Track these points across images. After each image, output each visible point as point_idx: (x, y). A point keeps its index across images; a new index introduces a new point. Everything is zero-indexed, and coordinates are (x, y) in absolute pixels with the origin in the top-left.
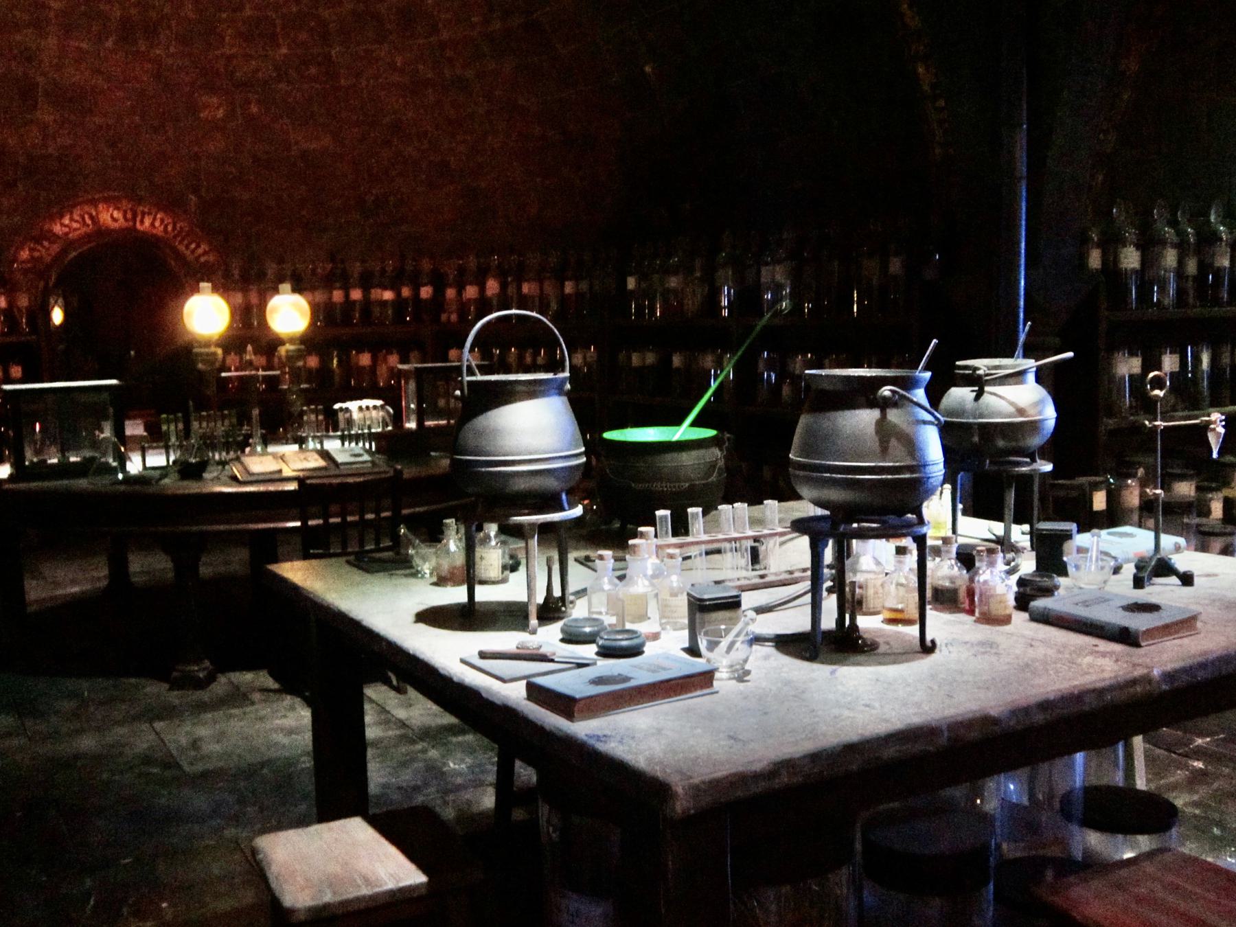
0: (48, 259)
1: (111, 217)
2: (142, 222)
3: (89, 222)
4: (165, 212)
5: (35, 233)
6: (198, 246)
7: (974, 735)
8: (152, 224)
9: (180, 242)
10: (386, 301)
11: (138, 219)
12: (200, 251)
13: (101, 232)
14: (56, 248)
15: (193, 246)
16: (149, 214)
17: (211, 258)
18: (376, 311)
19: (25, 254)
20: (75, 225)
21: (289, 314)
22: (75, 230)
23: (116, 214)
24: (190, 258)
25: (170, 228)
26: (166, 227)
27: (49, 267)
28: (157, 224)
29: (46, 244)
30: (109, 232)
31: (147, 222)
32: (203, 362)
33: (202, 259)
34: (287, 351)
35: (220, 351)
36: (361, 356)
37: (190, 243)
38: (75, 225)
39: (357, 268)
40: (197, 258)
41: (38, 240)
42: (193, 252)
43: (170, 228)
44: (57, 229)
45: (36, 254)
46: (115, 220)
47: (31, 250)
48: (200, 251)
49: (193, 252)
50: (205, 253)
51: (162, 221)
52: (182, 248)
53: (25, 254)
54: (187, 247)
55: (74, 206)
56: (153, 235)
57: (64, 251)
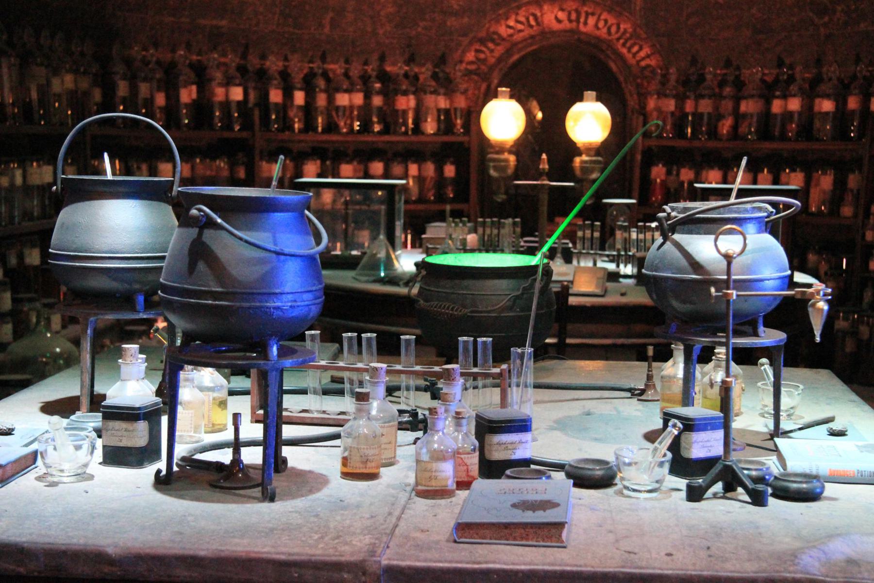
0: (492, 61)
1: (553, 17)
2: (585, 23)
3: (533, 23)
4: (609, 12)
5: (482, 34)
6: (641, 49)
7: (83, 570)
8: (596, 26)
9: (624, 45)
10: (827, 113)
11: (582, 20)
12: (642, 54)
13: (545, 33)
14: (499, 50)
15: (635, 49)
16: (593, 14)
17: (653, 62)
18: (817, 124)
19: (470, 56)
20: (520, 27)
21: (588, 122)
22: (520, 31)
23: (561, 15)
24: (633, 62)
25: (614, 29)
26: (609, 29)
27: (492, 68)
28: (601, 24)
29: (491, 45)
30: (553, 33)
31: (591, 21)
32: (496, 168)
33: (643, 64)
34: (583, 162)
35: (512, 158)
36: (793, 175)
37: (635, 44)
38: (520, 27)
39: (802, 74)
40: (638, 62)
41: (482, 41)
42: (634, 55)
43: (614, 29)
44: (503, 31)
45: (482, 56)
46: (559, 21)
47: (477, 51)
48: (642, 54)
49: (634, 55)
50: (648, 56)
51: (606, 21)
52: (624, 51)
53: (470, 56)
54: (629, 51)
55: (519, 7)
56: (598, 38)
57: (509, 52)
